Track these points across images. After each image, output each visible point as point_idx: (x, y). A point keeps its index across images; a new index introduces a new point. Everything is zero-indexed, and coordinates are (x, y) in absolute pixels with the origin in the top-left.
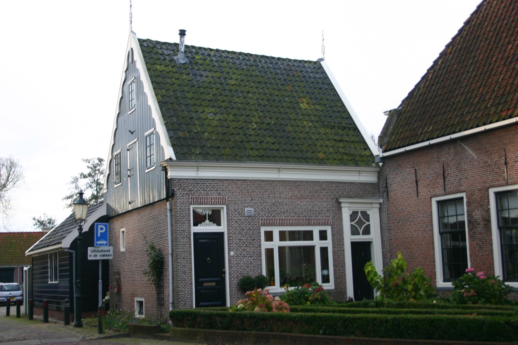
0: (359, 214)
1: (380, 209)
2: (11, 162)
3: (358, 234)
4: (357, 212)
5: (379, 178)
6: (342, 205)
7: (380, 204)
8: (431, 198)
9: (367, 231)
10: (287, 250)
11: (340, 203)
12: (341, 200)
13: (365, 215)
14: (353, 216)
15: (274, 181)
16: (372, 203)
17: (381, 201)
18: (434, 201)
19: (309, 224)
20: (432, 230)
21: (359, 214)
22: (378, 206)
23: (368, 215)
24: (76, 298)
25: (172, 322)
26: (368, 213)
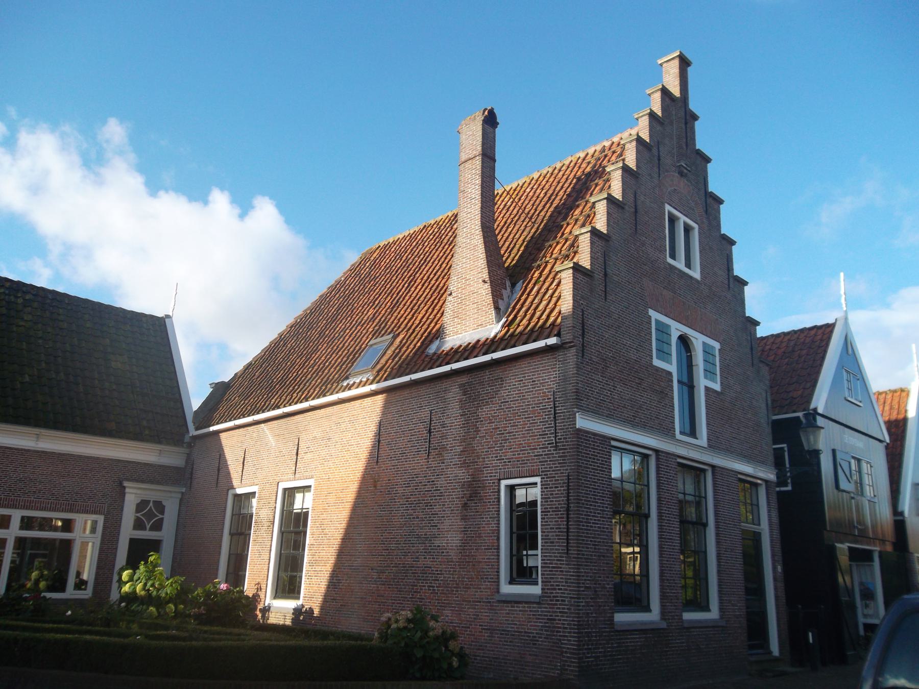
0: (151, 504)
1: (181, 500)
2: (438, 330)
3: (144, 528)
4: (148, 502)
5: (187, 462)
6: (127, 490)
7: (183, 493)
8: (500, 480)
9: (158, 526)
10: (57, 543)
11: (125, 488)
12: (126, 484)
13: (160, 507)
14: (141, 505)
15: (28, 451)
16: (170, 492)
17: (184, 490)
18: (504, 483)
19: (71, 511)
20: (222, 529)
21: (151, 504)
22: (179, 496)
23: (164, 507)
24: (535, 547)
25: (837, 579)
26: (164, 503)
